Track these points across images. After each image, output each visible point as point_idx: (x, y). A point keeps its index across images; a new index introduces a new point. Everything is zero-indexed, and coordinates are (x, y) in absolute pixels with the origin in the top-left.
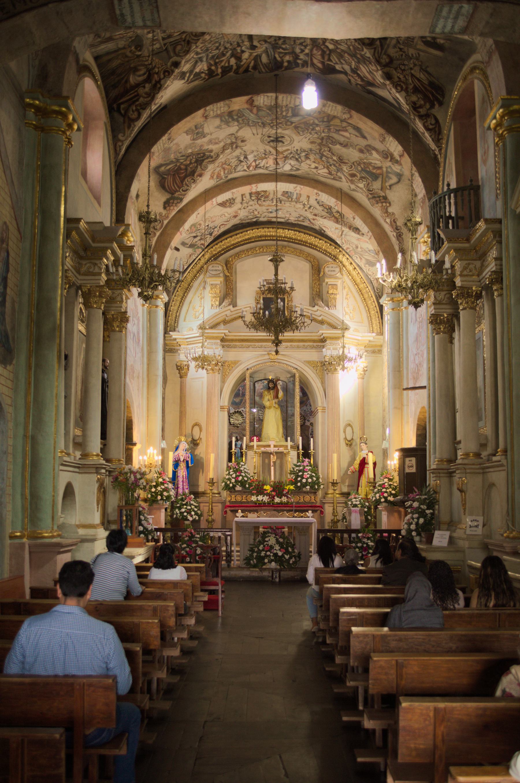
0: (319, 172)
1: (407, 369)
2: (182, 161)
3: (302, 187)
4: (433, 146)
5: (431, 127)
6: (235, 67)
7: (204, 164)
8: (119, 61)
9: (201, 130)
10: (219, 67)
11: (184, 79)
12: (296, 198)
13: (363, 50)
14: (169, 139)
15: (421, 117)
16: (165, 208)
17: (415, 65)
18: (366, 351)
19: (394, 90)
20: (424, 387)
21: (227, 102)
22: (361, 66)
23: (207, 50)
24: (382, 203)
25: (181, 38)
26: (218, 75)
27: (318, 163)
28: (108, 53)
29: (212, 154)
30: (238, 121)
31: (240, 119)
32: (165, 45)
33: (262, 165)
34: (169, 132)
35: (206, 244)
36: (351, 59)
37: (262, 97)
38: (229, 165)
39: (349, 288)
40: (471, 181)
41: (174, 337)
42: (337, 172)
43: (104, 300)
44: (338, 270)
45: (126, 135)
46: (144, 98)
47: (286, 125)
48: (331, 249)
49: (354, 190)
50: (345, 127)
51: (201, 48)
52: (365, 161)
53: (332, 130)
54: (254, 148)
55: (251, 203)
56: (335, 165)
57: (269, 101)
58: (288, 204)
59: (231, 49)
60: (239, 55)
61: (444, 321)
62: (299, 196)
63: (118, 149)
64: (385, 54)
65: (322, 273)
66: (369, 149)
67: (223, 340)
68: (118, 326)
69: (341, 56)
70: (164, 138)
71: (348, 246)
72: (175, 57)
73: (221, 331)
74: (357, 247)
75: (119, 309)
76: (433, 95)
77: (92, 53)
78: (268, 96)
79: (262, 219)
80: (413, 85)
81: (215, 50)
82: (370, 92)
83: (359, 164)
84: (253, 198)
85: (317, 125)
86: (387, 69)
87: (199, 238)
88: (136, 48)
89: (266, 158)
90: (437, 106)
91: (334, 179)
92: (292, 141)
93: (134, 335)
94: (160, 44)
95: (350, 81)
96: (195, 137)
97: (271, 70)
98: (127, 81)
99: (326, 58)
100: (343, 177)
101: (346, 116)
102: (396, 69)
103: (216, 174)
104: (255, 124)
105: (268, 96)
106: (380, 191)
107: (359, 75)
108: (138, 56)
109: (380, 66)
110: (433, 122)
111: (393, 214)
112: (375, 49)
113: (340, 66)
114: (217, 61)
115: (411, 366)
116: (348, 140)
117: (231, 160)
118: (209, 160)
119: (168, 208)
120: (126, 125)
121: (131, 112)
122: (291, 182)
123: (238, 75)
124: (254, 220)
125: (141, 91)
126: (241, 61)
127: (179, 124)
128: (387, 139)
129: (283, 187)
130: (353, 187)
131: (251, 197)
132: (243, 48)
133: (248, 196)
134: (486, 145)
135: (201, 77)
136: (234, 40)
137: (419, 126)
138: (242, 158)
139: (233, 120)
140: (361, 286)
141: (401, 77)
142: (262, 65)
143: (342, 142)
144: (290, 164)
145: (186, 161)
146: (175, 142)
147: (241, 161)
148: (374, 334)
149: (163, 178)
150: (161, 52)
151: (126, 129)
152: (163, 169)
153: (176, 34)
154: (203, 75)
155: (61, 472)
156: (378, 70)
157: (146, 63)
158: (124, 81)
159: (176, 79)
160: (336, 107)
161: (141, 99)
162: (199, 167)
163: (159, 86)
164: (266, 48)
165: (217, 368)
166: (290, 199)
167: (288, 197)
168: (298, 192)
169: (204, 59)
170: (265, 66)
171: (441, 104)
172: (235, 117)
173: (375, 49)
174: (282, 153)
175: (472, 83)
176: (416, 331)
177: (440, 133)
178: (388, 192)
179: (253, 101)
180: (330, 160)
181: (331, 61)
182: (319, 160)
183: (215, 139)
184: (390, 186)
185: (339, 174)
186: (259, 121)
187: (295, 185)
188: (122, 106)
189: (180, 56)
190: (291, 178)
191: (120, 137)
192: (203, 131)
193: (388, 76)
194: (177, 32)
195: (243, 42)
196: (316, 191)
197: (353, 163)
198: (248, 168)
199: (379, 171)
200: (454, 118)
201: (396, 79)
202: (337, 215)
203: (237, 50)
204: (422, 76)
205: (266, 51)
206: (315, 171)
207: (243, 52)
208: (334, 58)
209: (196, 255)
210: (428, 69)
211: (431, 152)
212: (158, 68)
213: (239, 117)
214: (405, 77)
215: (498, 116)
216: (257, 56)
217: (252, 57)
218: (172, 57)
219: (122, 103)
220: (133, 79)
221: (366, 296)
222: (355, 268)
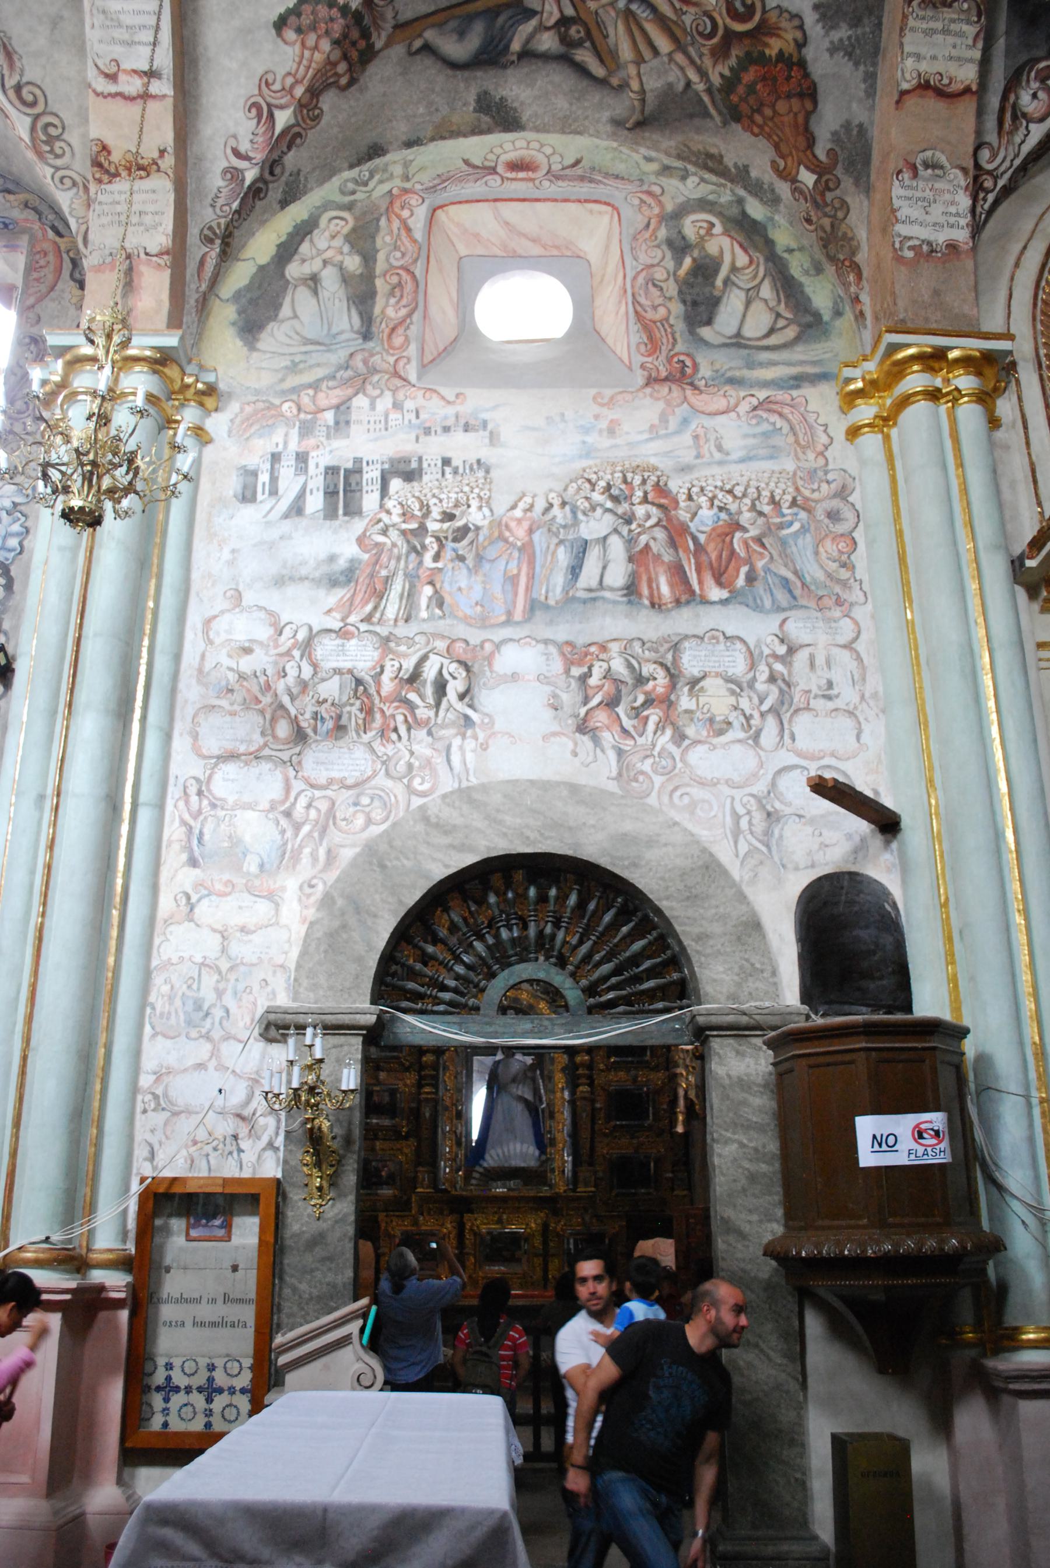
24: (345, 57)
106: (388, 26)
111: (317, 118)
178: (398, 50)
184: (428, 49)
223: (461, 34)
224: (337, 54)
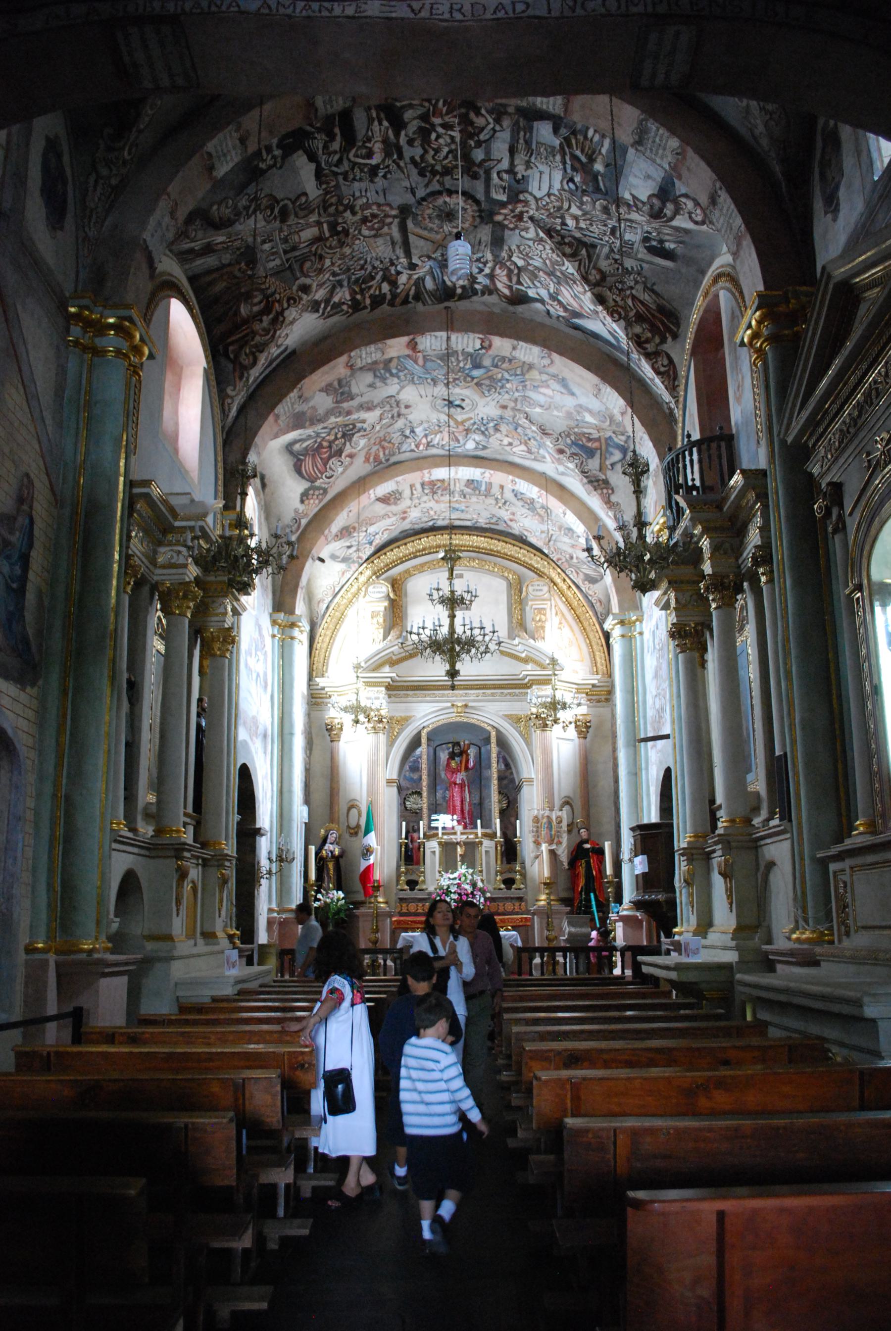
0: (514, 450)
1: (645, 717)
2: (323, 435)
3: (492, 472)
4: (666, 397)
5: (662, 369)
6: (389, 297)
7: (355, 438)
8: (224, 284)
9: (347, 389)
10: (367, 295)
11: (317, 311)
12: (486, 490)
13: (563, 264)
14: (300, 397)
15: (648, 356)
16: (302, 502)
17: (637, 282)
18: (589, 700)
19: (609, 319)
20: (667, 737)
21: (380, 345)
22: (562, 288)
23: (348, 270)
24: (602, 489)
25: (310, 251)
26: (365, 308)
27: (513, 438)
28: (209, 272)
29: (365, 426)
30: (398, 378)
31: (401, 374)
32: (288, 260)
33: (435, 442)
34: (299, 386)
35: (365, 557)
36: (548, 280)
37: (429, 337)
38: (390, 442)
39: (563, 615)
40: (721, 428)
41: (321, 685)
42: (539, 449)
43: (191, 604)
44: (546, 589)
45: (237, 388)
46: (261, 336)
47: (465, 381)
48: (536, 561)
49: (563, 474)
50: (546, 381)
51: (339, 266)
52: (576, 430)
53: (528, 387)
54: (423, 417)
55: (425, 498)
56: (535, 439)
57: (438, 344)
58: (474, 499)
59: (382, 269)
60: (393, 278)
61: (691, 633)
62: (489, 485)
63: (227, 408)
64: (594, 268)
65: (524, 594)
66: (580, 410)
67: (389, 688)
68: (219, 649)
69: (534, 276)
70: (292, 395)
71: (559, 556)
72: (303, 279)
73: (387, 673)
74: (572, 558)
75: (220, 624)
76: (663, 323)
77: (185, 272)
78: (436, 337)
79: (440, 523)
80: (635, 311)
81: (360, 269)
82: (577, 328)
83: (568, 435)
84: (426, 491)
85: (508, 381)
86: (598, 290)
87: (354, 549)
88: (247, 265)
89: (441, 432)
90: (670, 339)
91: (535, 459)
92: (474, 406)
93: (258, 675)
94: (281, 259)
95: (548, 312)
96: (339, 399)
97: (440, 301)
98: (237, 312)
99: (514, 279)
100: (547, 455)
101: (546, 362)
102: (610, 289)
103: (373, 454)
104: (422, 380)
105: (436, 337)
107: (560, 303)
109: (589, 285)
110: (666, 362)
111: (618, 504)
112: (580, 261)
113: (534, 290)
114: (363, 286)
115: (650, 713)
116: (549, 400)
117: (393, 435)
118: (361, 433)
119: (306, 502)
120: (237, 374)
121: (244, 356)
122: (476, 466)
123: (394, 309)
124: (431, 524)
125: (257, 327)
126: (397, 288)
127: (313, 375)
128: (603, 390)
129: (465, 473)
130: (561, 469)
131: (423, 489)
132: (399, 268)
133: (418, 487)
134: (740, 376)
135: (343, 310)
136: (386, 255)
137: (646, 370)
138: (407, 432)
139: (392, 375)
140: (579, 611)
141: (618, 299)
142: (427, 292)
143: (543, 404)
144: (474, 440)
145: (329, 435)
146: (311, 404)
147: (407, 437)
148: (599, 677)
149: (299, 460)
150: (283, 271)
151: (237, 379)
152: (297, 447)
153: (302, 245)
154: (345, 307)
155: (114, 853)
156: (585, 291)
157: (263, 287)
158: (231, 313)
159: (306, 310)
160: (530, 349)
161: (258, 338)
162: (348, 443)
163: (281, 319)
164: (431, 268)
165: (381, 725)
166: (477, 492)
167: (474, 489)
168: (487, 480)
169: (345, 283)
170: (431, 294)
171: (675, 336)
172: (394, 371)
173: (580, 261)
174: (462, 423)
175: (717, 296)
176: (655, 663)
177: (675, 377)
178: (609, 473)
179: (416, 343)
180: (528, 432)
181: (523, 285)
182: (514, 433)
183: (367, 403)
185: (542, 451)
186: (427, 376)
187: (482, 470)
188: (231, 348)
189: (310, 277)
190: (477, 460)
191: (229, 391)
192: (350, 390)
193: (600, 299)
194: (304, 242)
195: (398, 258)
196: (511, 477)
197: (560, 435)
198: (417, 446)
199: (596, 445)
200: (694, 352)
201: (612, 303)
202: (541, 512)
203: (390, 271)
204: (647, 297)
205: (431, 272)
206: (508, 448)
207: (399, 273)
208: (525, 279)
209: (351, 573)
210: (655, 287)
211: (665, 406)
212: (280, 294)
213: (400, 371)
215: (754, 323)
216: (418, 279)
217: (412, 282)
218: (298, 279)
219: (232, 343)
220: (244, 310)
221: (586, 624)
222: (570, 587)
223: (612, 454)
224: (599, 491)
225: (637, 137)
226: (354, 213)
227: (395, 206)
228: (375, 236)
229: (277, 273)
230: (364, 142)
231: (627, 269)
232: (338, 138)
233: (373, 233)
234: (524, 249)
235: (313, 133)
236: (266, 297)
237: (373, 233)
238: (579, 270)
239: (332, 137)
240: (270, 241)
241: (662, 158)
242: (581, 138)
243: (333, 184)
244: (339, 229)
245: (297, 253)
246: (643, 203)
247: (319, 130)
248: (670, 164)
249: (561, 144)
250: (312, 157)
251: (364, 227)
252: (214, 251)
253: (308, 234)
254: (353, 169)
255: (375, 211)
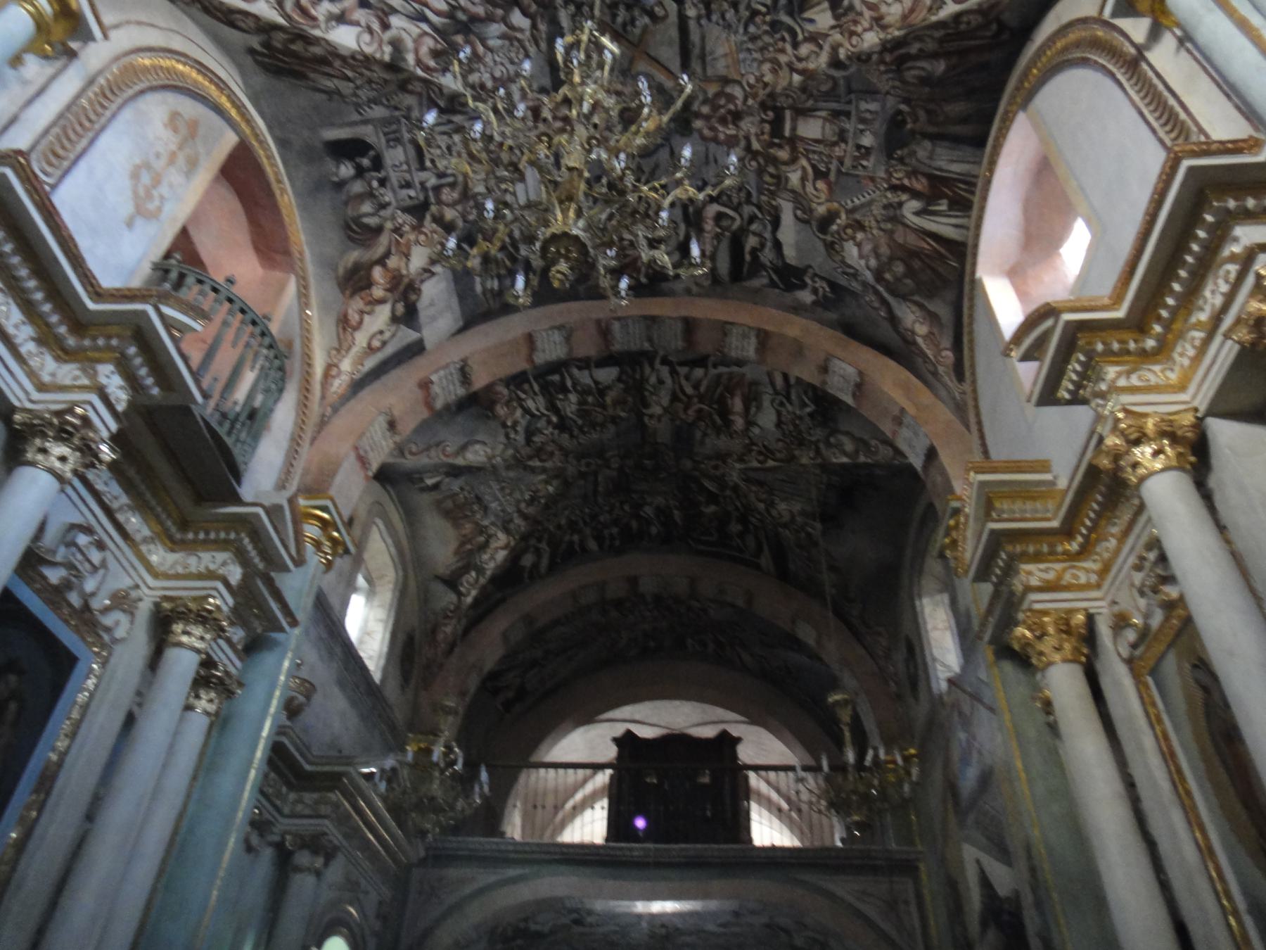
17: (355, 95)
28: (956, 140)
32: (849, 102)
51: (783, 51)
86: (401, 76)
88: (904, 122)
94: (857, 107)
102: (386, 81)
108: (907, 101)
125: (931, 46)
150: (861, 91)
153: (823, 114)
156: (419, 62)
157: (897, 83)
194: (820, 117)
195: (699, 18)
214: (361, 74)
218: (846, 78)
220: (940, 67)
225: (467, 369)
226: (747, 138)
227: (696, 135)
228: (726, 81)
229: (870, 92)
230: (722, 234)
231: (376, 104)
232: (748, 248)
233: (728, 90)
234: (517, 53)
235: (772, 269)
236: (899, 71)
237: (728, 90)
238: (440, 88)
239: (754, 251)
240: (859, 147)
241: (440, 379)
242: (503, 272)
243: (764, 198)
244: (771, 114)
245: (834, 105)
246: (422, 281)
247: (763, 267)
248: (432, 382)
249: (517, 249)
250: (778, 245)
251: (739, 103)
252: (930, 177)
253: (811, 129)
254: (740, 204)
255: (721, 129)
